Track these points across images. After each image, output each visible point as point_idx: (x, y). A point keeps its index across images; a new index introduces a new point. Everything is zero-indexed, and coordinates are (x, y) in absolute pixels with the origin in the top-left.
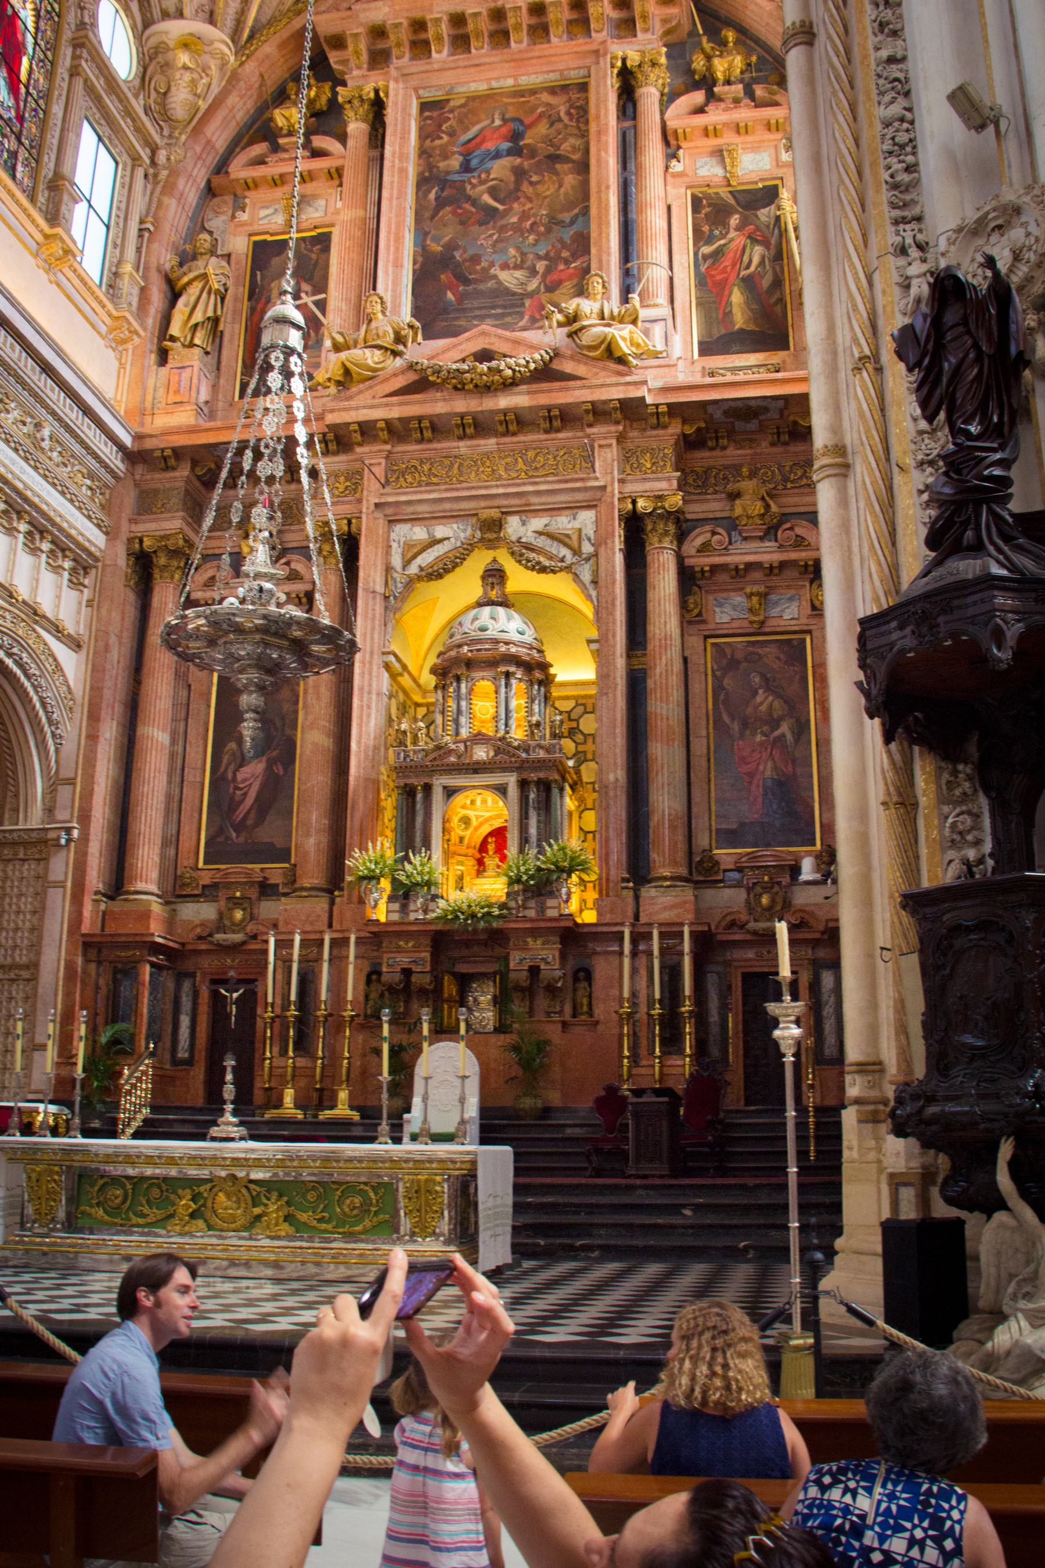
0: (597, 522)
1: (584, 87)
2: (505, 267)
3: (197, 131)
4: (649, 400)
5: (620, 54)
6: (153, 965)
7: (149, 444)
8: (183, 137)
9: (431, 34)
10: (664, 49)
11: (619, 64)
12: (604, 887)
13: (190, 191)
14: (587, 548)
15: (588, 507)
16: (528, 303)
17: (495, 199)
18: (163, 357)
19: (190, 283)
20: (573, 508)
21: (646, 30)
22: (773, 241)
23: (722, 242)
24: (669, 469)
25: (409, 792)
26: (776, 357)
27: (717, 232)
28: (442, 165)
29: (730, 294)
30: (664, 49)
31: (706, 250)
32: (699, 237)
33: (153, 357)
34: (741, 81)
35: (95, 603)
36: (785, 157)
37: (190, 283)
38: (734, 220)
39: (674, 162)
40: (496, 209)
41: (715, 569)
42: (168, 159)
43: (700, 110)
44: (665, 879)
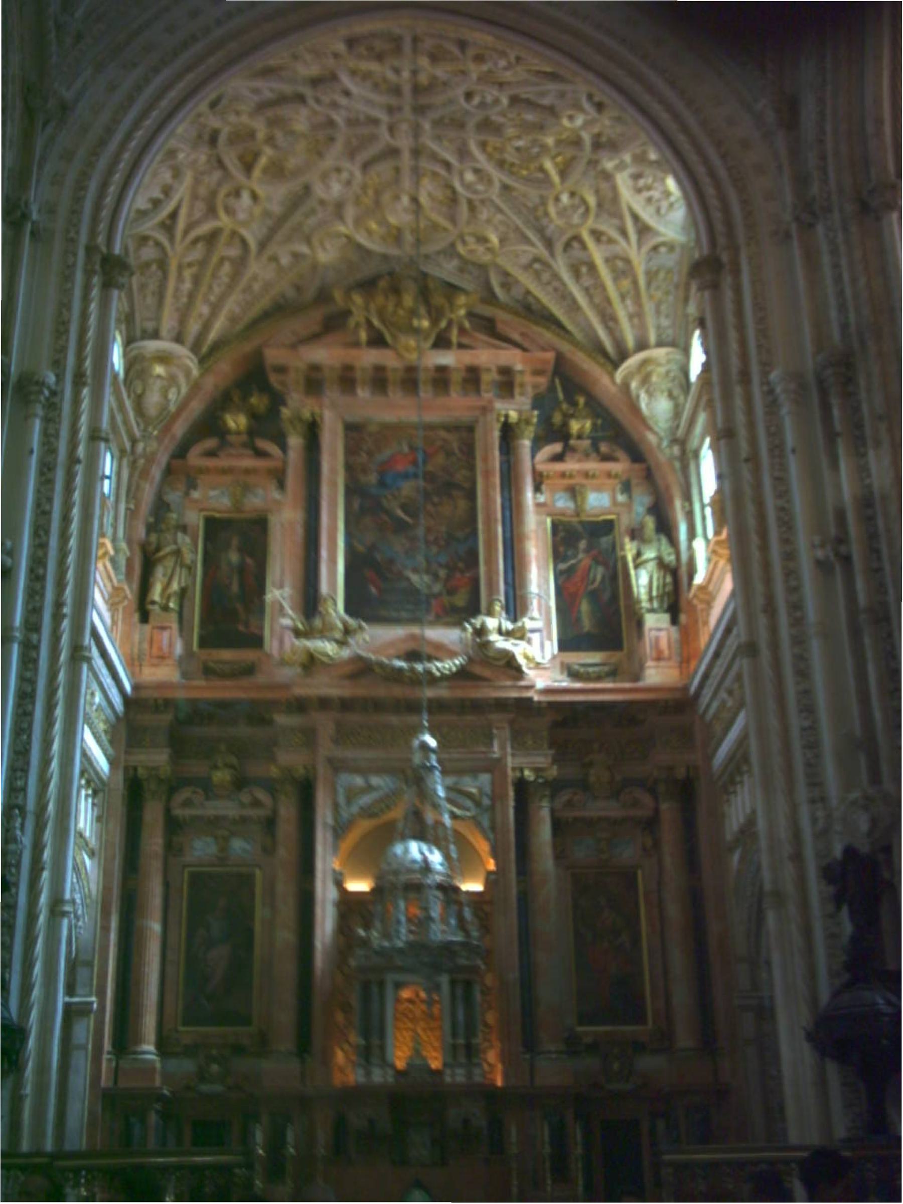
0: (493, 783)
1: (471, 429)
2: (415, 570)
3: (166, 429)
4: (536, 698)
5: (503, 412)
6: (157, 1112)
7: (144, 694)
8: (155, 433)
9: (358, 375)
10: (536, 413)
11: (502, 419)
12: (504, 1057)
13: (156, 473)
14: (486, 802)
15: (487, 770)
16: (433, 602)
17: (406, 512)
18: (145, 618)
19: (165, 557)
20: (474, 772)
21: (522, 394)
22: (611, 564)
23: (573, 562)
24: (545, 746)
25: (366, 987)
26: (615, 657)
27: (570, 553)
28: (363, 479)
29: (580, 603)
30: (536, 413)
31: (562, 566)
32: (558, 556)
33: (136, 617)
34: (588, 438)
35: (104, 820)
36: (621, 498)
37: (165, 557)
38: (583, 544)
39: (538, 495)
40: (406, 523)
41: (576, 819)
42: (144, 449)
43: (558, 458)
44: (550, 1052)
